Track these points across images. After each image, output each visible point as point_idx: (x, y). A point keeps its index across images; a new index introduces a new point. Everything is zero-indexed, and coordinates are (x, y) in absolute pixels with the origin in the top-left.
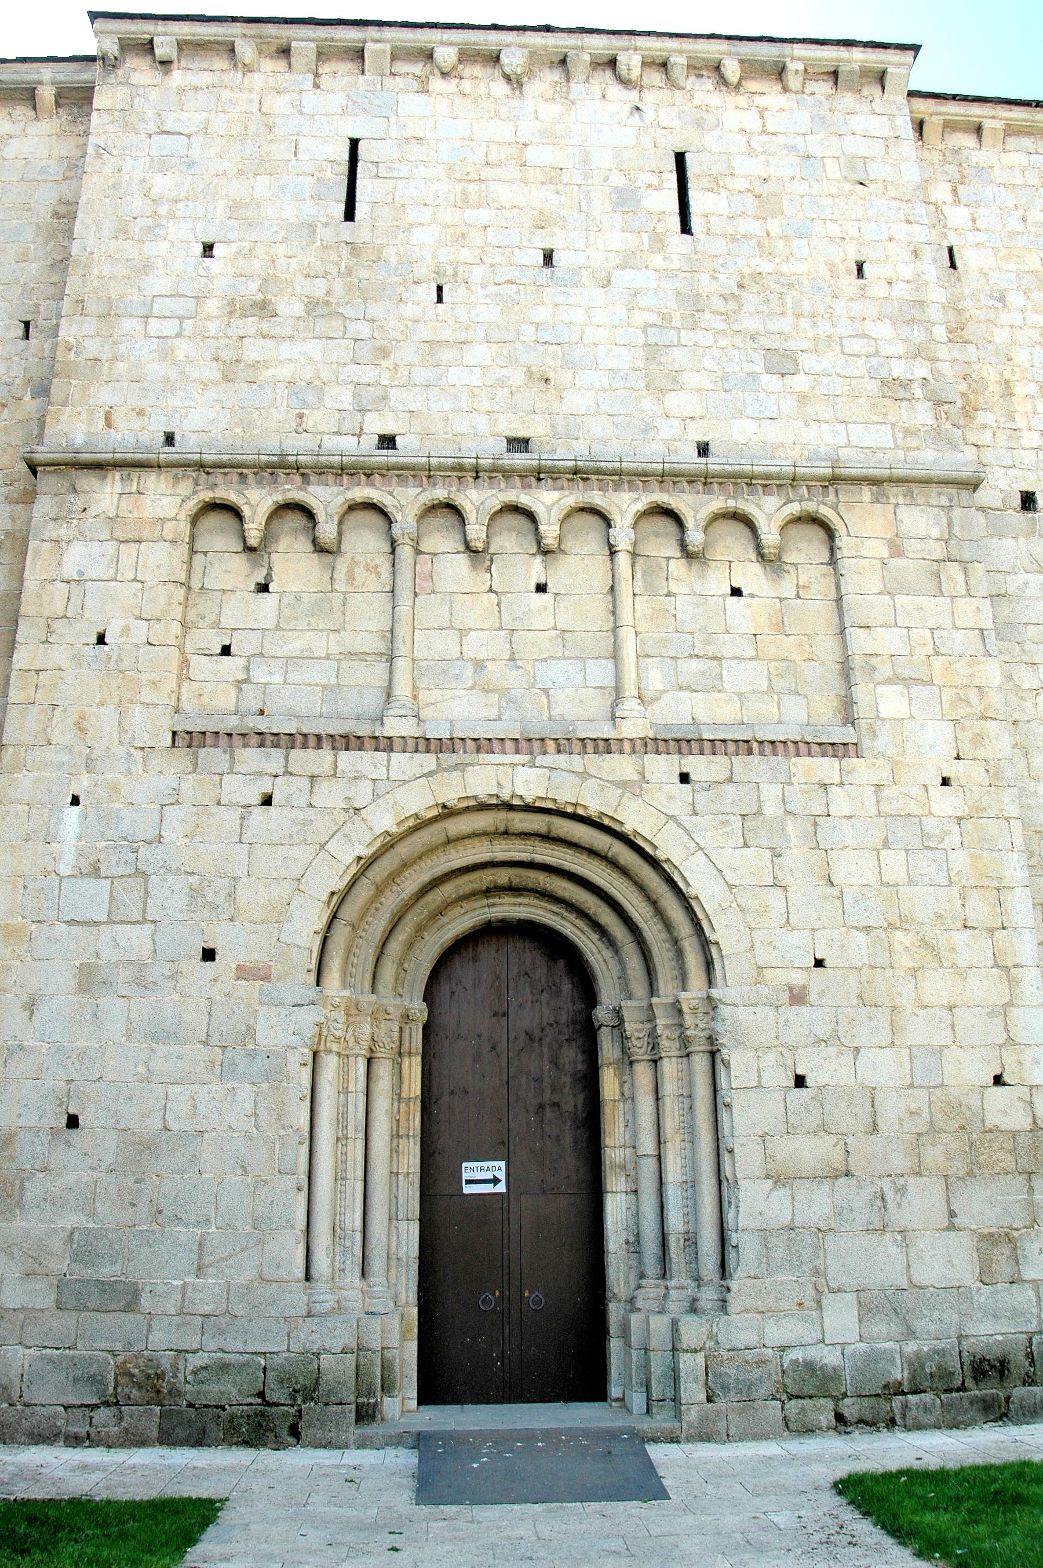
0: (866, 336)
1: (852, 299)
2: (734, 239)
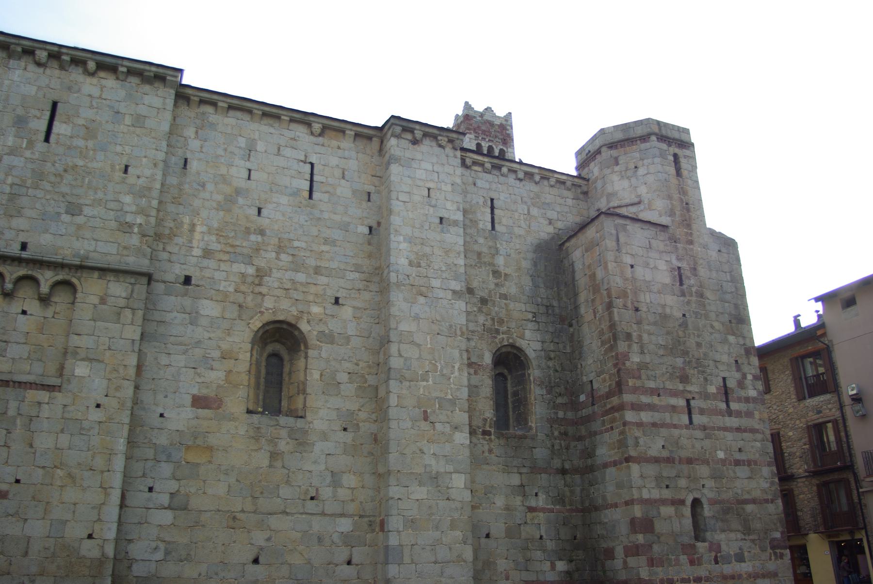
0: (119, 201)
1: (117, 183)
2: (69, 148)
